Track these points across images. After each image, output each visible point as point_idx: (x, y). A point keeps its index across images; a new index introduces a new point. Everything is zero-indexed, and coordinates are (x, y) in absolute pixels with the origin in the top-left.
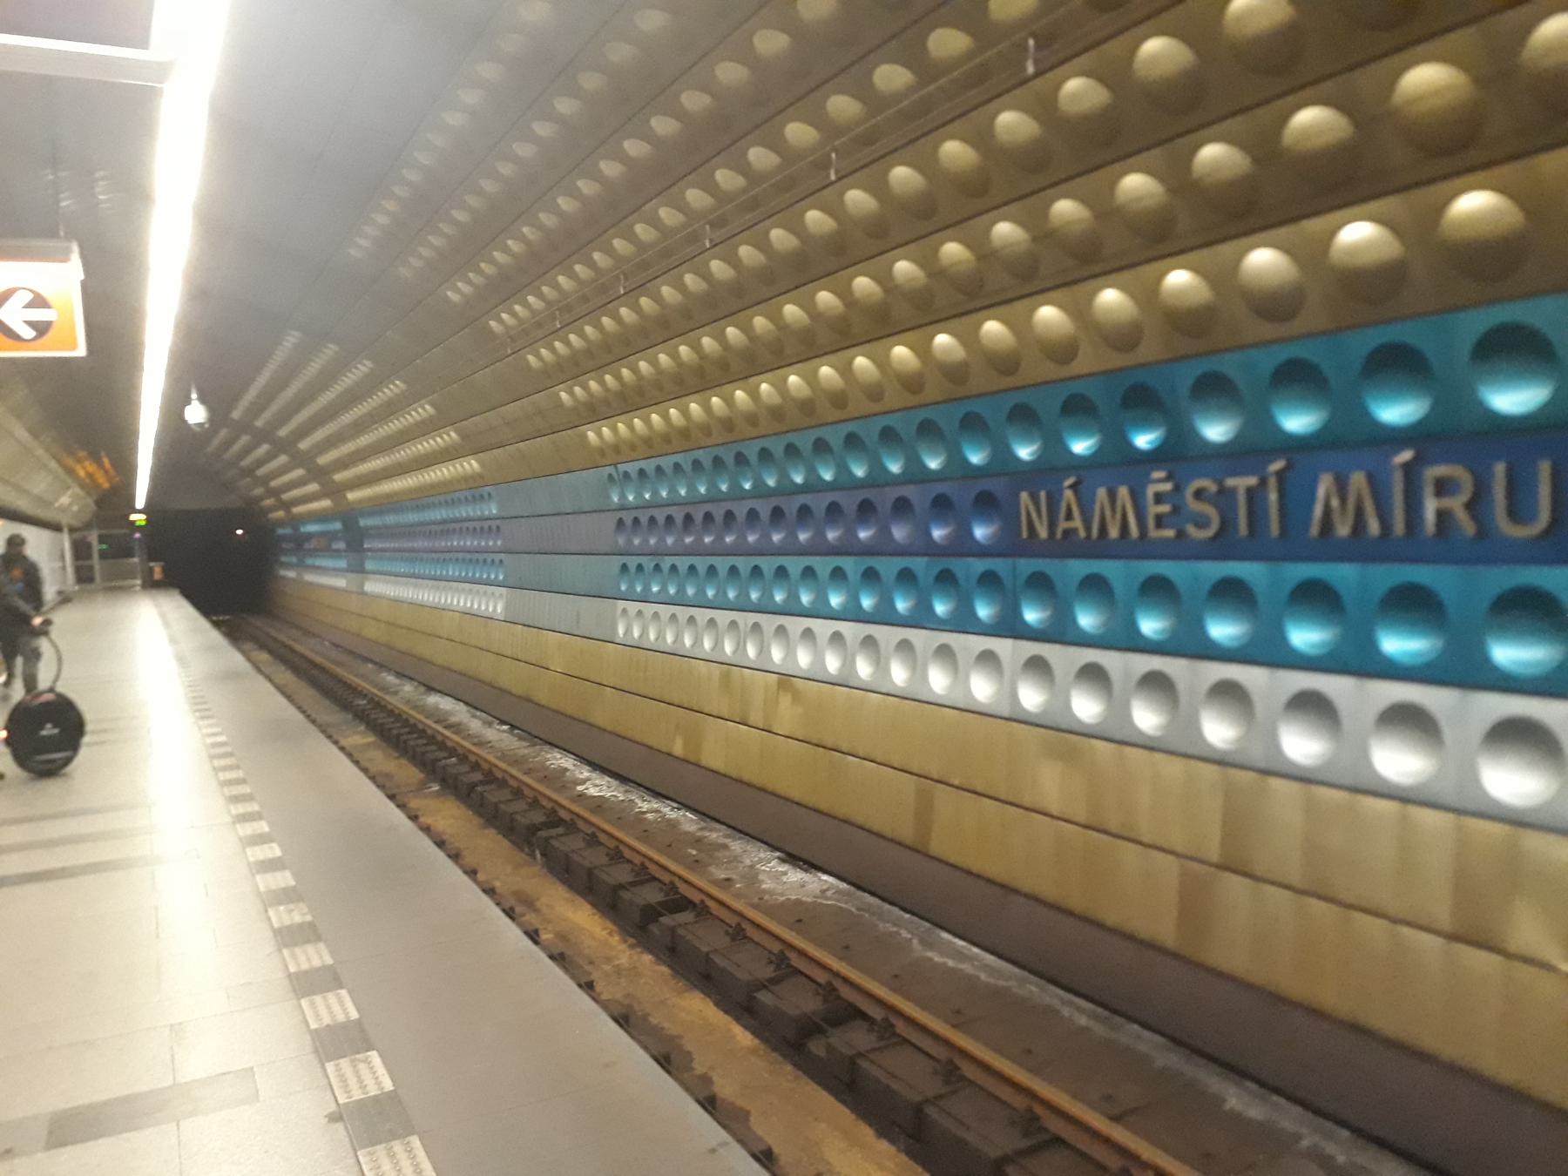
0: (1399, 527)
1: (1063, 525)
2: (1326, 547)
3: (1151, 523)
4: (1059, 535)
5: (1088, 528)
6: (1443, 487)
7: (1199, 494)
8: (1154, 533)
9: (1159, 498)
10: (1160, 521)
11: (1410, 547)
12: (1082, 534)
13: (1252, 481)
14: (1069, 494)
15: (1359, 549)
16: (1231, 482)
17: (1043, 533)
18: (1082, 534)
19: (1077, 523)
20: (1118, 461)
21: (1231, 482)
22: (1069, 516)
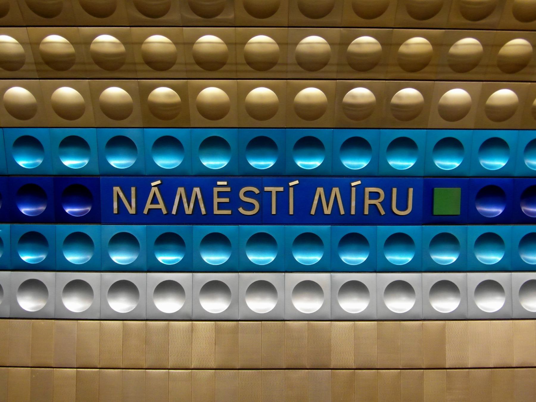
0: (353, 212)
1: (149, 205)
2: (320, 218)
3: (215, 206)
4: (146, 212)
5: (169, 207)
6: (374, 196)
7: (246, 194)
8: (216, 212)
9: (221, 195)
10: (221, 206)
11: (360, 219)
12: (165, 212)
13: (281, 189)
14: (155, 190)
15: (335, 219)
16: (267, 189)
17: (132, 211)
18: (165, 212)
19: (161, 205)
20: (239, 176)
21: (267, 189)
22: (155, 201)
